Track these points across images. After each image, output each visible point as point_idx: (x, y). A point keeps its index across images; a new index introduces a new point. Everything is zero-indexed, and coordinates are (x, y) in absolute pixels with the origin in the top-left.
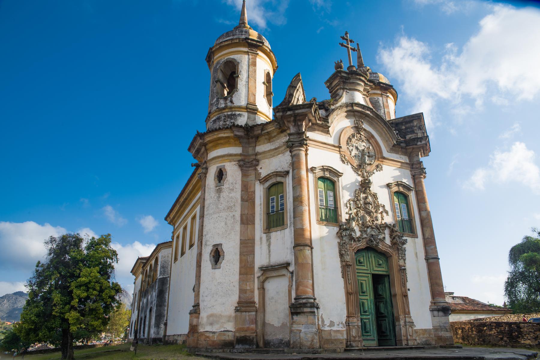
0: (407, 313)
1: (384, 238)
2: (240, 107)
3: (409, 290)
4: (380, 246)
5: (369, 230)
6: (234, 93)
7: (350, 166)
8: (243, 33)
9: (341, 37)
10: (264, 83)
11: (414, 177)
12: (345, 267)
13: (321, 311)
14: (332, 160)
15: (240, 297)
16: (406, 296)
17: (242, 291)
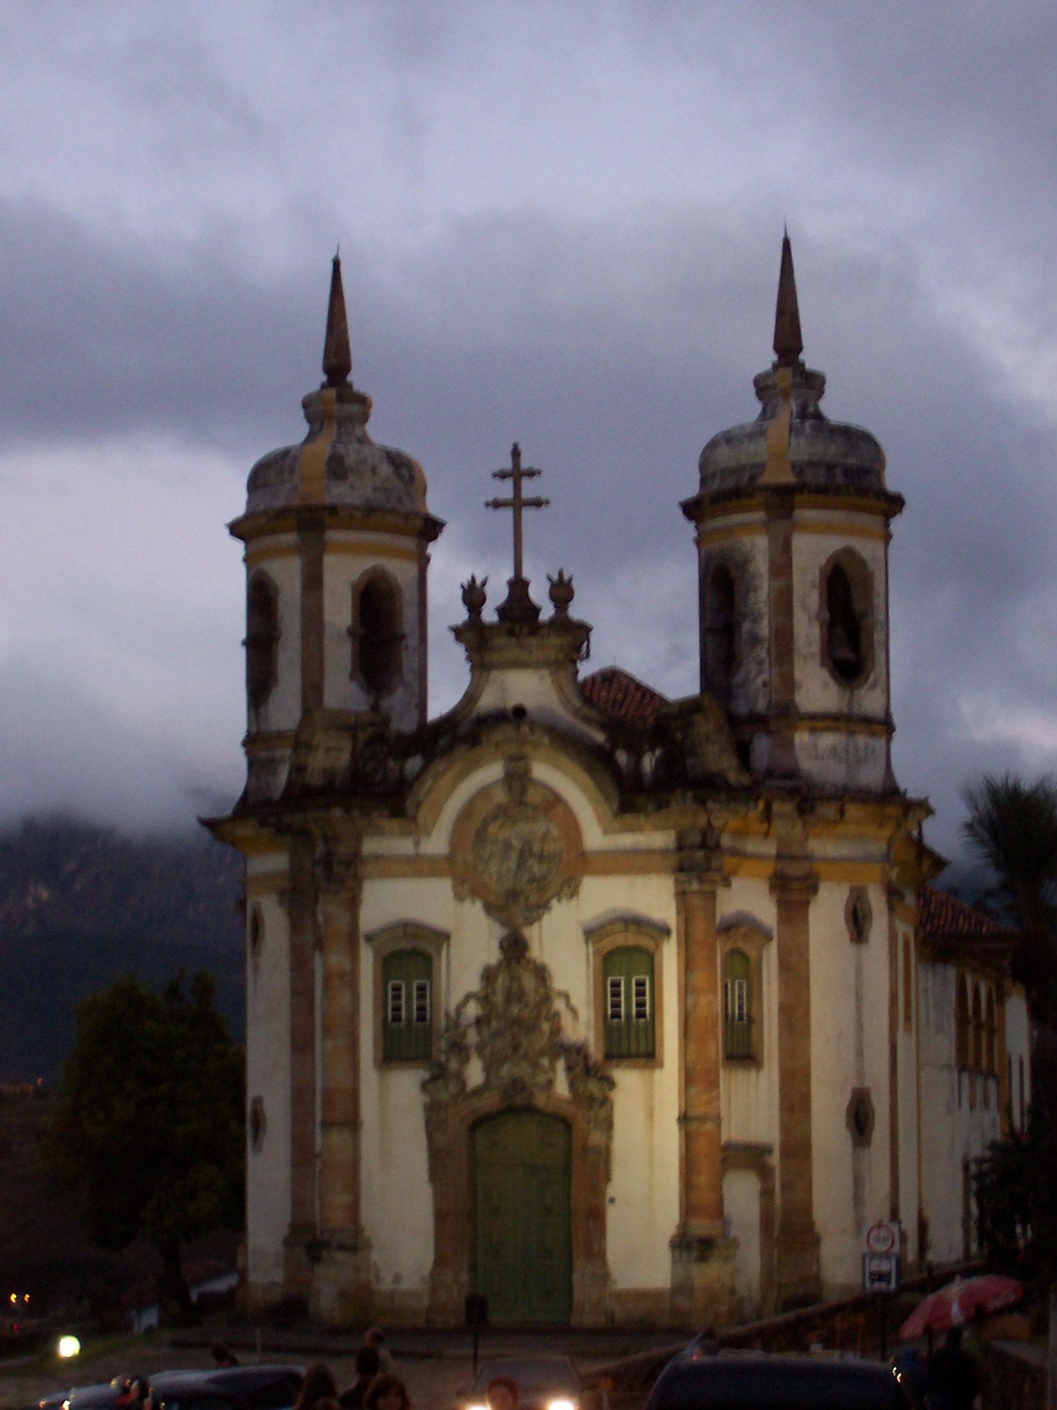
0: (597, 1254)
1: (551, 1083)
2: (280, 735)
3: (612, 1200)
4: (540, 1100)
5: (505, 1069)
6: (269, 693)
7: (479, 905)
8: (286, 476)
9: (495, 475)
10: (351, 633)
11: (681, 895)
12: (437, 1157)
13: (375, 1257)
14: (425, 900)
15: (293, 1214)
16: (597, 1216)
17: (298, 1202)
